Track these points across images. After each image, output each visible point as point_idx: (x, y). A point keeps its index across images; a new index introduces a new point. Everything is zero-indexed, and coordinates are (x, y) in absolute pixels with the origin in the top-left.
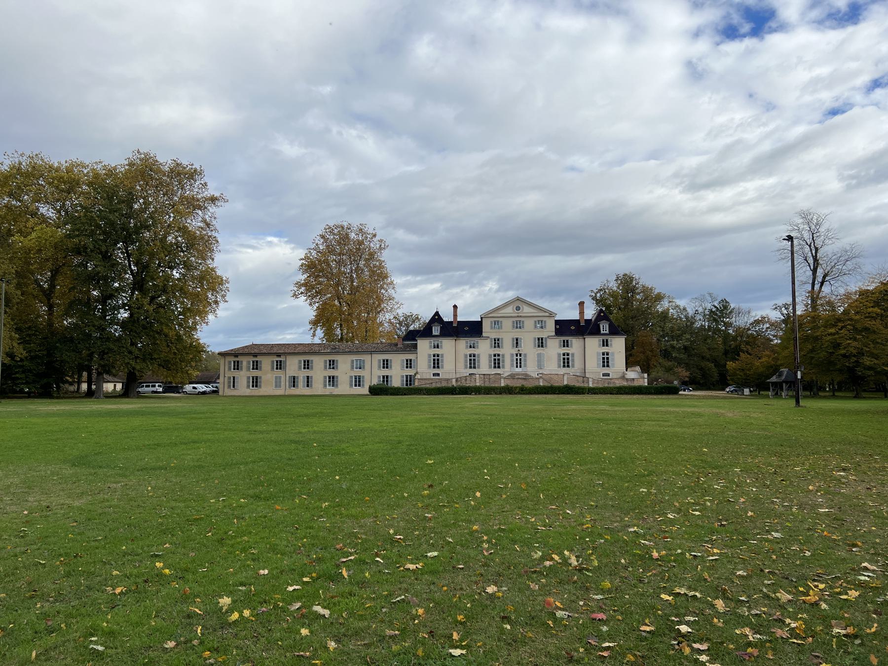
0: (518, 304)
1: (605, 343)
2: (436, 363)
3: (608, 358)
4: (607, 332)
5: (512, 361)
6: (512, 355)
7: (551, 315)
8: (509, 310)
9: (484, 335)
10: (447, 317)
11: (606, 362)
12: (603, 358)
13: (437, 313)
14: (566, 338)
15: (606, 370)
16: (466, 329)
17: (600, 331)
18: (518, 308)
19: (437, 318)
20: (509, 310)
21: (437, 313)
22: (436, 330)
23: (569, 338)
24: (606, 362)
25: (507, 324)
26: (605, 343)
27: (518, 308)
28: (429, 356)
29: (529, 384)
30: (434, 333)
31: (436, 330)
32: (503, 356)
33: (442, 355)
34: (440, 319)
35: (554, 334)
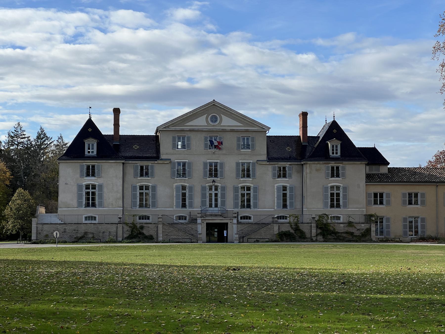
2: (91, 198)
5: (203, 196)
6: (203, 188)
7: (264, 129)
9: (163, 156)
10: (106, 128)
14: (282, 164)
18: (214, 119)
21: (90, 124)
22: (91, 147)
23: (287, 164)
25: (198, 143)
27: (214, 119)
28: (80, 187)
32: (191, 189)
33: (101, 186)
35: (265, 157)
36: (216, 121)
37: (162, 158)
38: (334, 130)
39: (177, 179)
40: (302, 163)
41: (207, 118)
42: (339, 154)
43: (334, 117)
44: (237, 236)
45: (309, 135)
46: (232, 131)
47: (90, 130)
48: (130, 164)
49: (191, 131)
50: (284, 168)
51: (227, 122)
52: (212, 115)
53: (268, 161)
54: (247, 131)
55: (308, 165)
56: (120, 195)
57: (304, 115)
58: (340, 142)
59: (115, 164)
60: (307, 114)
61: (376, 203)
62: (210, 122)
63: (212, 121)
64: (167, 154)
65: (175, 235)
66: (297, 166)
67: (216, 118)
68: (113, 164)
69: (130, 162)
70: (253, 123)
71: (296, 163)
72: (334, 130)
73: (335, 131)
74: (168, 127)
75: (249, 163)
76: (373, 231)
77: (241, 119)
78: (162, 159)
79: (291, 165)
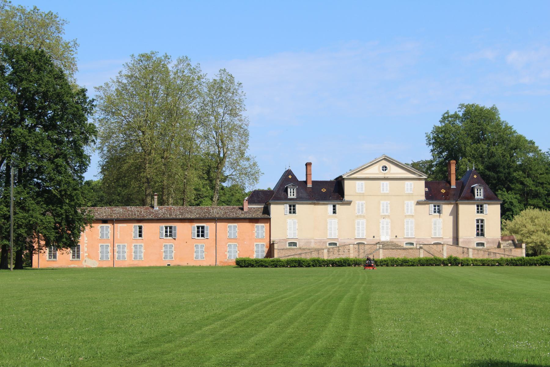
0: (385, 163)
1: (480, 210)
3: (482, 226)
4: (482, 197)
9: (346, 198)
11: (480, 232)
12: (478, 226)
13: (289, 172)
15: (481, 240)
16: (324, 190)
17: (474, 196)
18: (385, 168)
19: (288, 178)
21: (289, 172)
24: (480, 232)
26: (480, 210)
27: (385, 168)
29: (411, 256)
30: (289, 197)
31: (292, 193)
34: (294, 177)
35: (423, 198)
36: (385, 170)
47: (290, 177)
63: (383, 170)
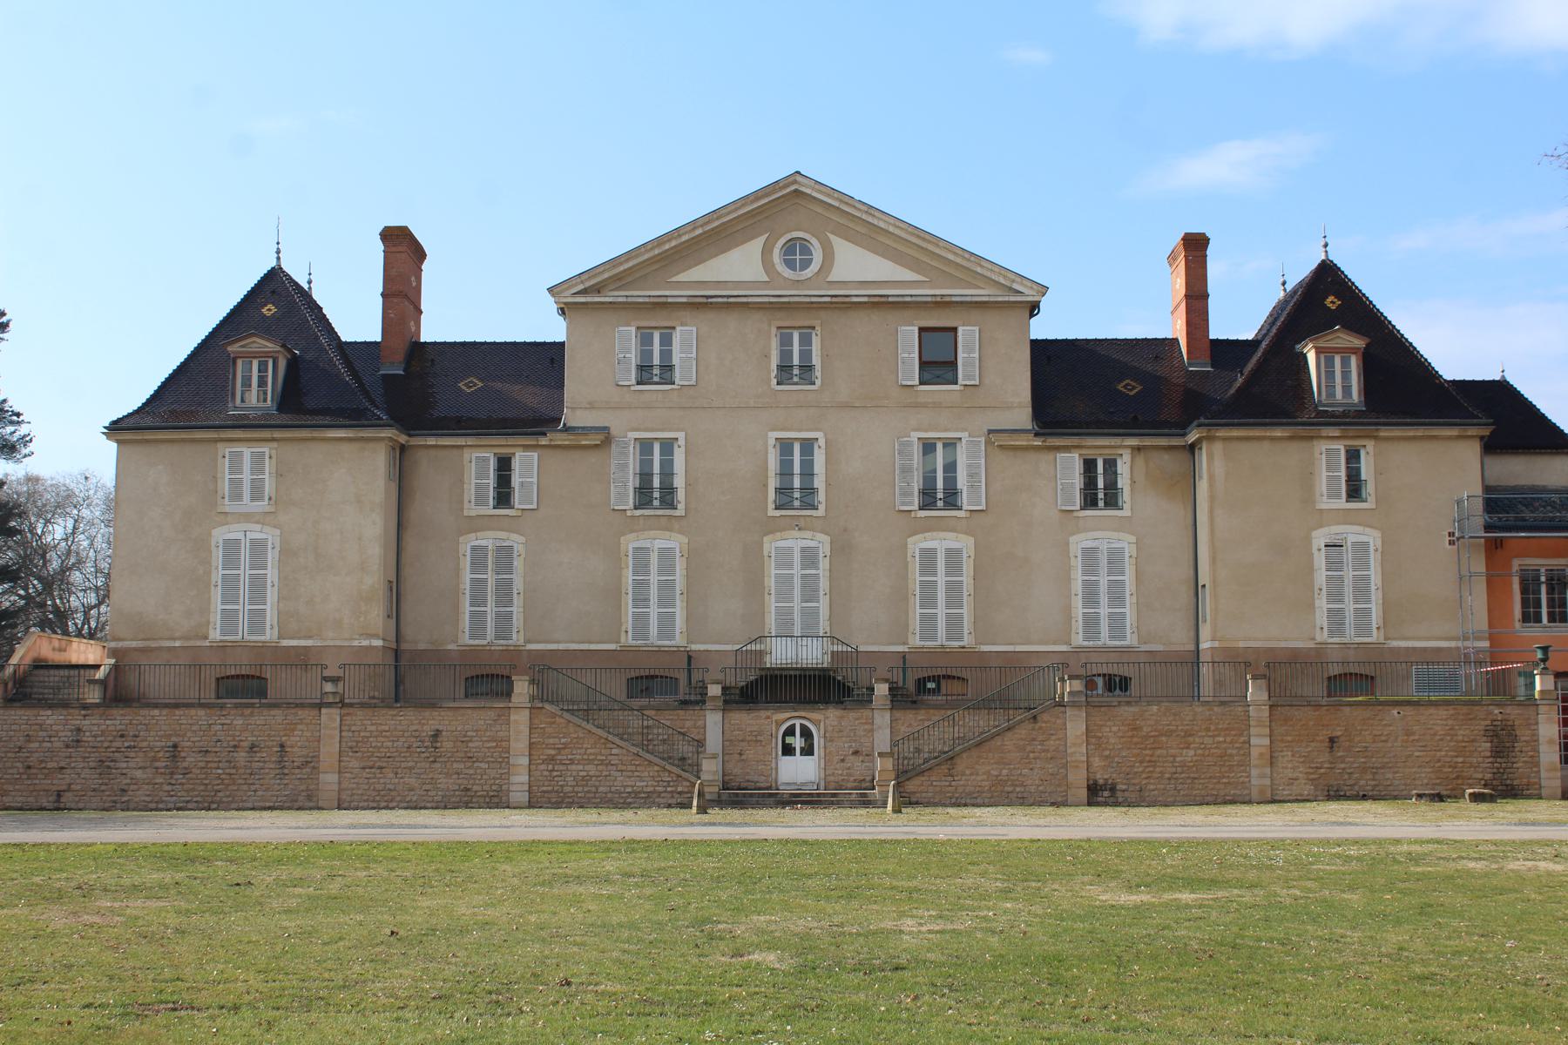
8: (740, 266)
9: (571, 417)
10: (356, 316)
14: (1099, 446)
18: (796, 253)
20: (740, 266)
21: (275, 285)
27: (796, 253)
35: (1021, 415)
36: (806, 264)
37: (571, 424)
38: (1326, 300)
39: (638, 512)
40: (1192, 437)
41: (766, 252)
42: (1356, 395)
43: (1326, 245)
44: (889, 763)
45: (1216, 332)
46: (880, 304)
47: (269, 310)
48: (433, 452)
49: (699, 305)
50: (1111, 464)
51: (856, 266)
52: (789, 236)
53: (1036, 435)
54: (942, 304)
55: (1218, 447)
56: (374, 578)
57: (1195, 246)
58: (1359, 342)
59: (354, 447)
60: (1207, 240)
61: (1531, 616)
62: (781, 268)
63: (790, 264)
64: (592, 406)
65: (590, 762)
66: (1166, 456)
67: (806, 250)
68: (345, 447)
69: (431, 441)
70: (967, 265)
71: (1163, 442)
72: (1326, 300)
73: (1332, 302)
74: (598, 289)
75: (950, 445)
76: (1550, 742)
77: (916, 255)
78: (566, 429)
79: (1138, 449)
